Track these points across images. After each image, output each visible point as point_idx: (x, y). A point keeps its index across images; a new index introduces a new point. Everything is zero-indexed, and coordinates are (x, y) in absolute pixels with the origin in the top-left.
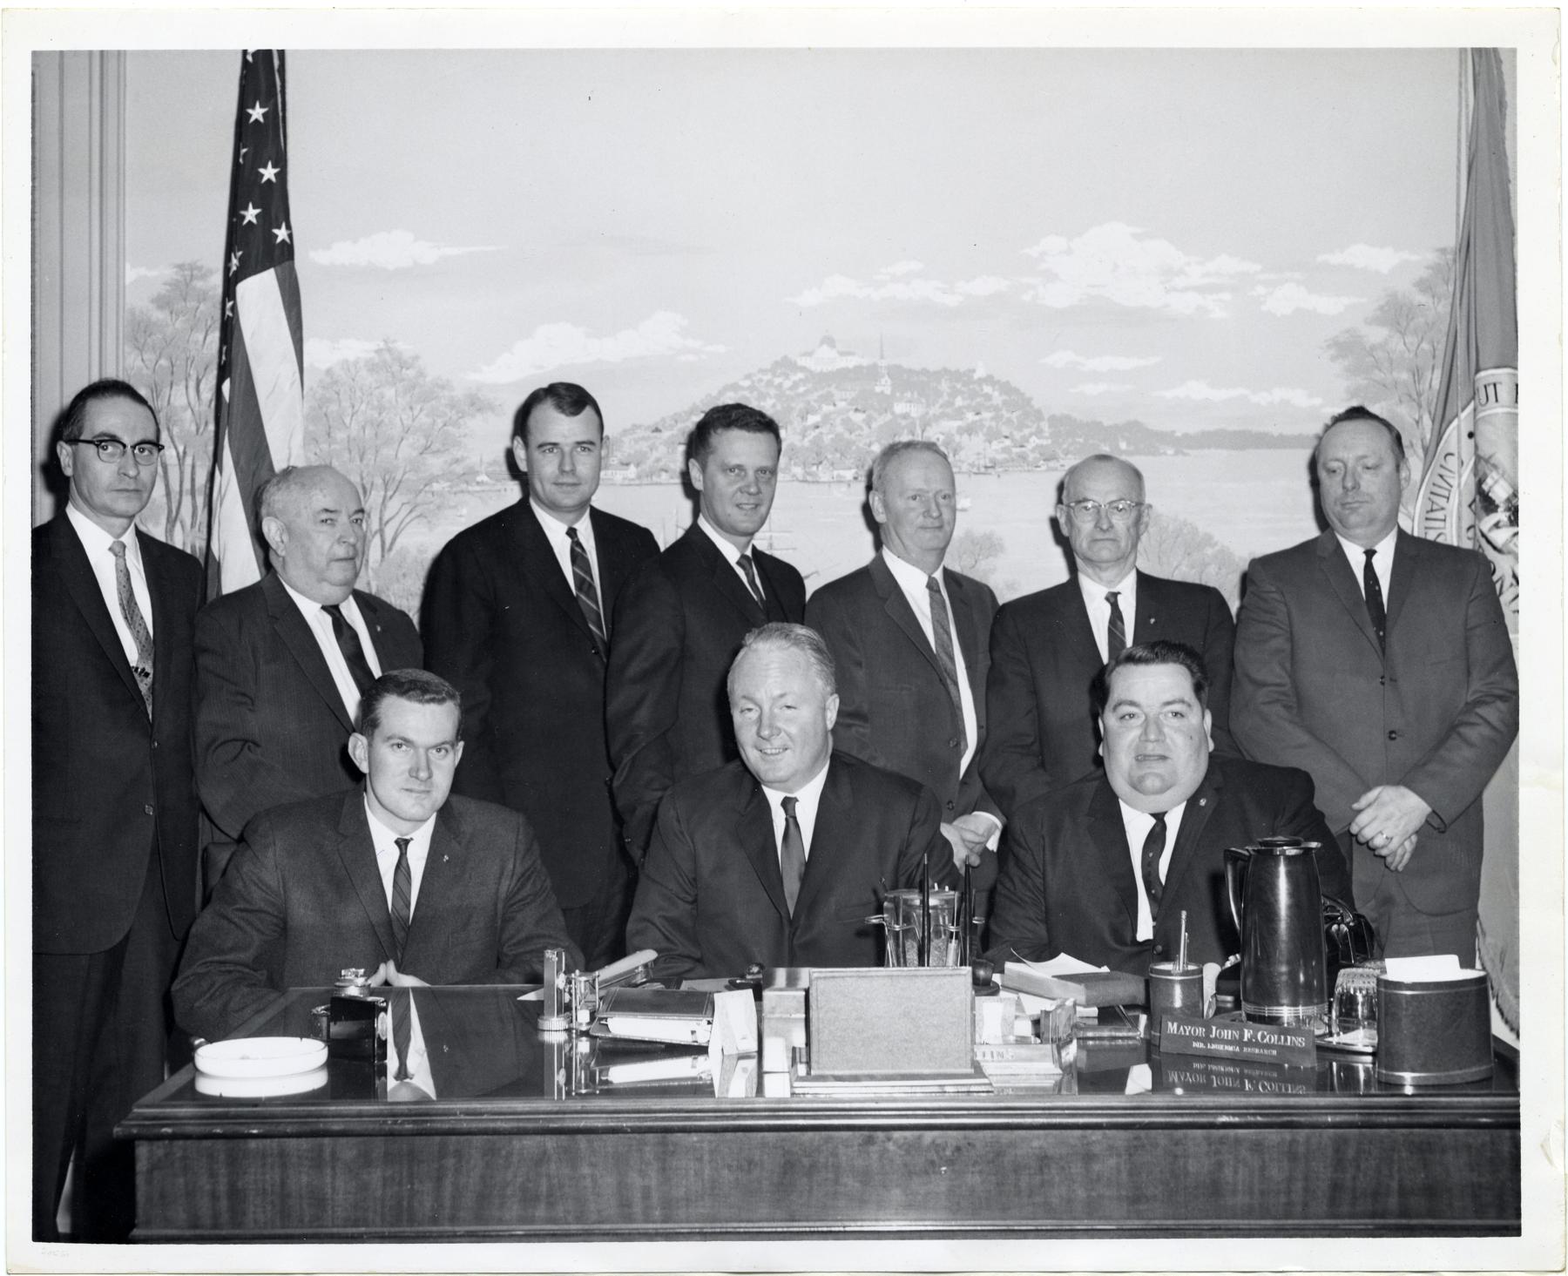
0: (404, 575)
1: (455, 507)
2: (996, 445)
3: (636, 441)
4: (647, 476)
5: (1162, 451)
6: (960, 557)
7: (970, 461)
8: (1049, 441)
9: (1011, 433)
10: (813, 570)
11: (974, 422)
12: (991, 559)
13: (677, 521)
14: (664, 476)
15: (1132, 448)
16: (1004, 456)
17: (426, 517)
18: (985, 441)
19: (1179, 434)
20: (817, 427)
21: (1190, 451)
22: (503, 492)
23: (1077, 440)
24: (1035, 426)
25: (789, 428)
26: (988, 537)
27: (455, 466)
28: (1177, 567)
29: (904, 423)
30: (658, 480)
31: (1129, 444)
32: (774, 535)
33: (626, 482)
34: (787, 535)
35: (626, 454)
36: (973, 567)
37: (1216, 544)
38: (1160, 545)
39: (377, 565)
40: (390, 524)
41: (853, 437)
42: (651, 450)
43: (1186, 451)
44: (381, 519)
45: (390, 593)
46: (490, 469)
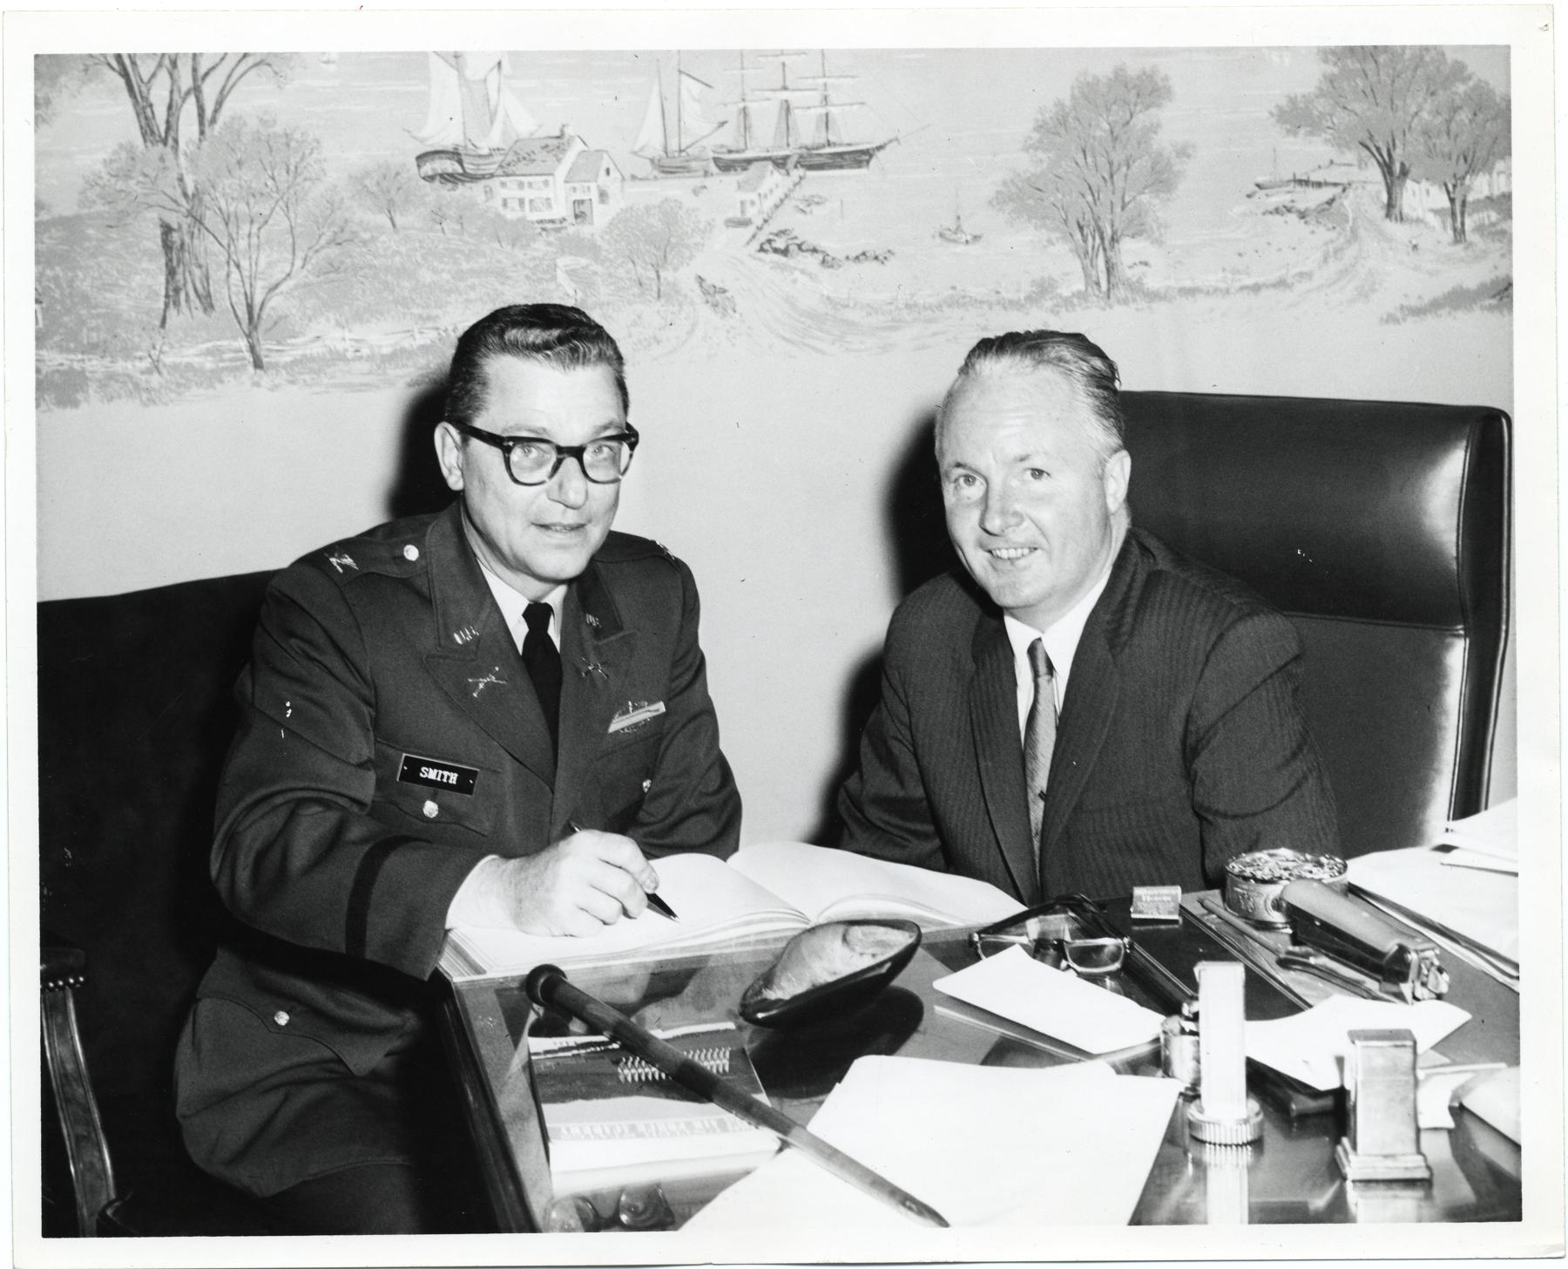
0: (239, 163)
10: (891, 137)
12: (1153, 111)
13: (679, 61)
17: (269, 65)
28: (1416, 114)
32: (830, 81)
34: (850, 81)
36: (1128, 123)
37: (1470, 78)
38: (1393, 81)
39: (192, 148)
40: (209, 80)
44: (195, 70)
45: (218, 195)
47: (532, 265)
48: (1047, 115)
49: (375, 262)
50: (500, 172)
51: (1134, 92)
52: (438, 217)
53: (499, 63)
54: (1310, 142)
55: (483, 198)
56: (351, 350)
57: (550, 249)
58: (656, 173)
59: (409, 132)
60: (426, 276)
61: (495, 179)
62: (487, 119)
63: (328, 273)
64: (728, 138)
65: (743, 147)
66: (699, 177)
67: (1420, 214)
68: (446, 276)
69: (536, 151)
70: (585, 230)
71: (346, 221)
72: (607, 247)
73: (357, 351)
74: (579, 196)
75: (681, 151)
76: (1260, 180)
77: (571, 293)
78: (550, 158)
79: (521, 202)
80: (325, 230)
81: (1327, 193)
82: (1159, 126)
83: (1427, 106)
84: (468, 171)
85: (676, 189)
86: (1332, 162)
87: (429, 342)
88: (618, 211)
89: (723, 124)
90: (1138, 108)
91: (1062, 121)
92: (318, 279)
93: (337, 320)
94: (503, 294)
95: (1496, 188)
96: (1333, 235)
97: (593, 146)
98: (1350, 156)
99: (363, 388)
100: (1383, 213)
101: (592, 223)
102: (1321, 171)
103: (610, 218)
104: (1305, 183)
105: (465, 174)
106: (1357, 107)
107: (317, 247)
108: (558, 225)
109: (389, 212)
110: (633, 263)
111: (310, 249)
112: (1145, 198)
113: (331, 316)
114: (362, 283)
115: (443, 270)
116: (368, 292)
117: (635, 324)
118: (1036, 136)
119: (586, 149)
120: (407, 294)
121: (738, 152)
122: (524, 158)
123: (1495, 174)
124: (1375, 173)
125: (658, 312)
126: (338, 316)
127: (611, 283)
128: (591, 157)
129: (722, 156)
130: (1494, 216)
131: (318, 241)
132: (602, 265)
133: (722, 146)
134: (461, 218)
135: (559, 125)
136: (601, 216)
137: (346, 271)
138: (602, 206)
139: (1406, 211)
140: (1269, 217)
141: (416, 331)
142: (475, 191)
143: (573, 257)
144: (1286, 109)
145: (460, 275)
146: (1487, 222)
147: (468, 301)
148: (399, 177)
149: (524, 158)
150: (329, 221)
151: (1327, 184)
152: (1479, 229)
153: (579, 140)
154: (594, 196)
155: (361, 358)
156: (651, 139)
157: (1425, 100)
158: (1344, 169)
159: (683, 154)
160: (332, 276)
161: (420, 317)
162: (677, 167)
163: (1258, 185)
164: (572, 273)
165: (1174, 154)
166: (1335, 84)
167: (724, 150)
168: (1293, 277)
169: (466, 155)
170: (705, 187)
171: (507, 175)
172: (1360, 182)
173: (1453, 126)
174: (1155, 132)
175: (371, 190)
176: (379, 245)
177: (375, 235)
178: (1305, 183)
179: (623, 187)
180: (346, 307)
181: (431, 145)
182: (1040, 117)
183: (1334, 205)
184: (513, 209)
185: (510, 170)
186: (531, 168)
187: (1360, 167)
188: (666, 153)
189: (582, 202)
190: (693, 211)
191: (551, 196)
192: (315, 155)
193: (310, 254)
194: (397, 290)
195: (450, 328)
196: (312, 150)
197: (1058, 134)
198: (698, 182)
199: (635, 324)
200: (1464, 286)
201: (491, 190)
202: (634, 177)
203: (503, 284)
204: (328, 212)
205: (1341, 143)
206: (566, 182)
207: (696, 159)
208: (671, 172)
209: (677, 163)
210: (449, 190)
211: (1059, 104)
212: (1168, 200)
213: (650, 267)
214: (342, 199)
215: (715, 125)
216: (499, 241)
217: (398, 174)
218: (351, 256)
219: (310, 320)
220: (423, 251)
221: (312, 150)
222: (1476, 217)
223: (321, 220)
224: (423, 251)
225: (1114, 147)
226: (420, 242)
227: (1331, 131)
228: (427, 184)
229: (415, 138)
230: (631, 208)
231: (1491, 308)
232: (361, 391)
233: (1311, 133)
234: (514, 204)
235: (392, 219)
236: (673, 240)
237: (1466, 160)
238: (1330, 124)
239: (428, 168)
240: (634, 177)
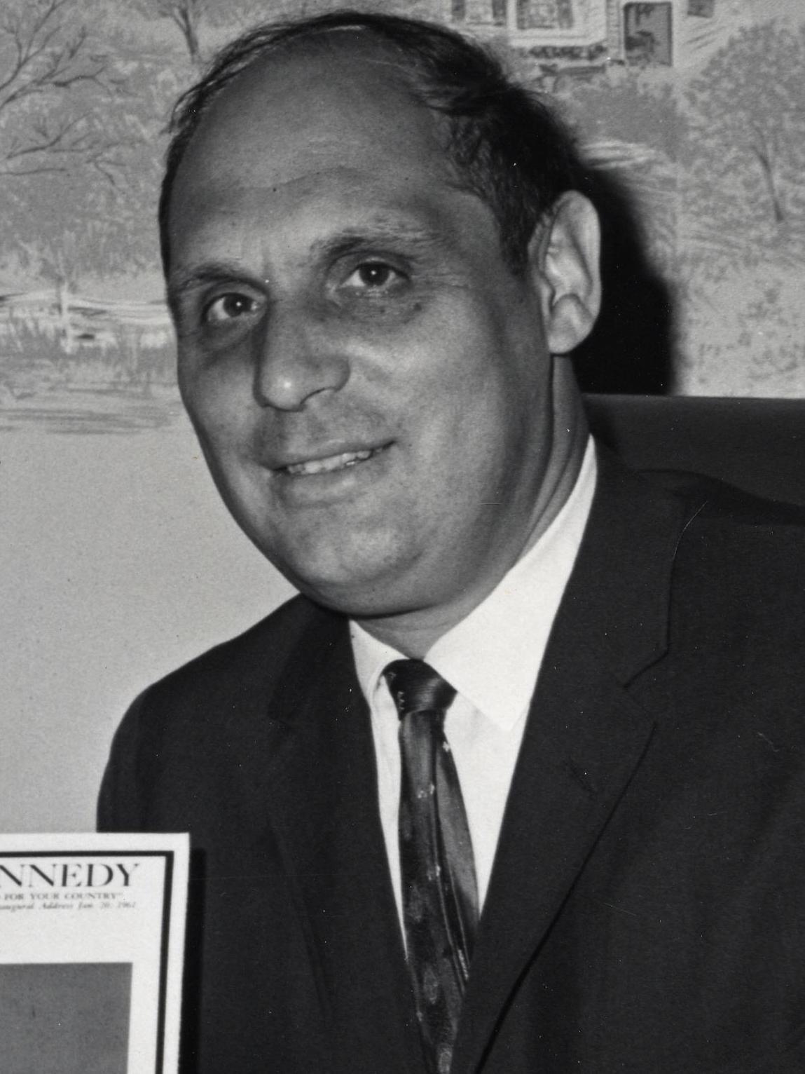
56: (72, 332)
63: (35, 150)
70: (652, 77)
72: (702, 120)
73: (87, 337)
80: (33, 50)
88: (737, 35)
92: (11, 165)
93: (45, 261)
99: (95, 425)
101: (668, 63)
103: (709, 51)
107: (13, 89)
108: (585, 63)
109: (185, 16)
110: (765, 162)
113: (32, 250)
116: (120, 200)
117: (759, 312)
126: (47, 250)
127: (706, 211)
131: (16, 73)
132: (687, 163)
138: (695, 20)
143: (617, 143)
150: (44, 29)
155: (95, 352)
160: (41, 157)
176: (152, 87)
177: (147, 66)
184: (477, 20)
199: (759, 312)
218: (88, 115)
230: (768, 29)
235: (188, 33)
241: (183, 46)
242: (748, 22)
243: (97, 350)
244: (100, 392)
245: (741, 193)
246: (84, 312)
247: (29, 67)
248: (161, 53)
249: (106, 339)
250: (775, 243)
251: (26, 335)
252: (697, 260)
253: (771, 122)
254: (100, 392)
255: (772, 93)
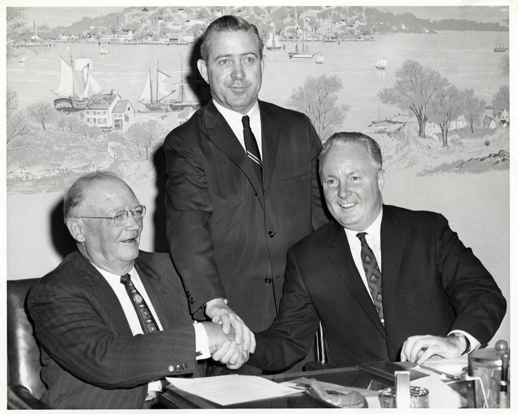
1: (17, 56)
2: (338, 25)
3: (133, 16)
4: (140, 39)
5: (423, 31)
6: (318, 91)
7: (324, 34)
8: (366, 24)
9: (346, 18)
11: (325, 10)
12: (335, 92)
14: (150, 38)
15: (408, 29)
16: (342, 31)
18: (331, 22)
19: (431, 21)
20: (240, 11)
21: (438, 32)
22: (49, 45)
23: (380, 23)
24: (358, 14)
25: (223, 10)
26: (334, 79)
27: (17, 28)
29: (288, 10)
30: (147, 42)
31: (406, 27)
33: (127, 42)
35: (126, 25)
37: (449, 84)
41: (260, 18)
42: (142, 22)
43: (435, 31)
46: (40, 31)
47: (98, 145)
48: (296, 93)
49: (36, 142)
50: (87, 108)
51: (328, 85)
52: (61, 124)
53: (88, 65)
54: (392, 106)
55: (80, 118)
57: (105, 139)
58: (147, 110)
59: (52, 91)
60: (56, 148)
61: (85, 110)
62: (83, 86)
64: (176, 97)
65: (181, 101)
66: (164, 112)
67: (431, 136)
68: (64, 148)
69: (101, 100)
70: (119, 132)
71: (25, 126)
72: (128, 138)
73: (27, 178)
74: (117, 118)
75: (157, 102)
76: (374, 120)
77: (113, 156)
78: (106, 102)
79: (95, 120)
81: (397, 126)
82: (337, 98)
83: (434, 94)
84: (74, 107)
85: (155, 116)
86: (399, 114)
87: (56, 174)
89: (175, 91)
90: (329, 91)
91: (302, 95)
92: (13, 149)
94: (86, 156)
95: (458, 126)
96: (400, 142)
97: (123, 99)
98: (406, 112)
100: (418, 134)
102: (395, 118)
103: (129, 127)
104: (390, 122)
105: (73, 108)
106: (409, 94)
108: (109, 129)
109: (43, 122)
111: (10, 136)
112: (331, 125)
113: (17, 163)
114: (30, 150)
115: (63, 146)
116: (32, 154)
117: (137, 169)
118: (291, 100)
119: (119, 99)
120: (48, 155)
121: (179, 103)
122: (97, 103)
123: (458, 121)
124: (415, 119)
125: (147, 164)
128: (123, 103)
129: (173, 104)
130: (458, 137)
132: (125, 145)
133: (173, 100)
134: (71, 125)
135: (111, 90)
136: (126, 126)
137: (24, 145)
138: (126, 122)
139: (426, 133)
140: (376, 134)
141: (51, 170)
142: (77, 115)
144: (383, 93)
145: (69, 148)
146: (455, 139)
147: (73, 159)
148: (47, 109)
149: (97, 103)
150: (18, 125)
151: (398, 123)
152: (452, 141)
153: (117, 96)
154: (123, 118)
156: (146, 96)
157: (433, 92)
158: (405, 116)
159: (158, 103)
160: (18, 147)
161: (53, 165)
162: (156, 108)
163: (373, 122)
164: (113, 148)
165: (342, 109)
166: (401, 85)
167: (174, 102)
168: (386, 157)
169: (74, 101)
170: (166, 116)
171: (90, 109)
172: (409, 122)
173: (443, 102)
174: (336, 101)
175: (36, 113)
178: (390, 122)
179: (134, 115)
180: (24, 160)
181: (61, 96)
182: (293, 93)
183: (400, 130)
184: (91, 123)
185: (91, 106)
186: (99, 107)
187: (410, 115)
188: (152, 101)
189: (118, 120)
190: (161, 125)
191: (106, 117)
192: (14, 99)
193: (10, 138)
194: (44, 153)
195: (65, 169)
196: (13, 97)
197: (299, 100)
198: (163, 114)
200: (447, 163)
201: (83, 115)
202: (139, 111)
203: (86, 152)
204: (18, 121)
205: (403, 108)
206: (112, 112)
207: (163, 105)
208: (155, 110)
209: (156, 106)
210: (67, 114)
211: (300, 88)
212: (340, 126)
213: (144, 147)
214: (24, 117)
215: (171, 92)
216: (85, 135)
217: (46, 107)
219: (9, 165)
220: (56, 138)
221: (13, 97)
222: (451, 137)
223: (15, 125)
224: (56, 138)
225: (320, 106)
226: (55, 135)
227: (399, 102)
228: (58, 112)
229: (54, 93)
230: (137, 123)
231: (457, 172)
232: (28, 194)
233: (392, 103)
234: (92, 120)
235: (43, 125)
236: (153, 137)
237: (448, 116)
238: (399, 100)
239: (59, 106)
240: (139, 111)
241: (43, 128)
242: (134, 123)
243: (29, 180)
244: (30, 187)
245: (134, 150)
246: (27, 173)
247: (16, 132)
248: (39, 129)
249: (30, 178)
250: (139, 158)
251: (16, 178)
252: (127, 161)
253: (138, 138)
254: (30, 187)
255: (138, 134)
